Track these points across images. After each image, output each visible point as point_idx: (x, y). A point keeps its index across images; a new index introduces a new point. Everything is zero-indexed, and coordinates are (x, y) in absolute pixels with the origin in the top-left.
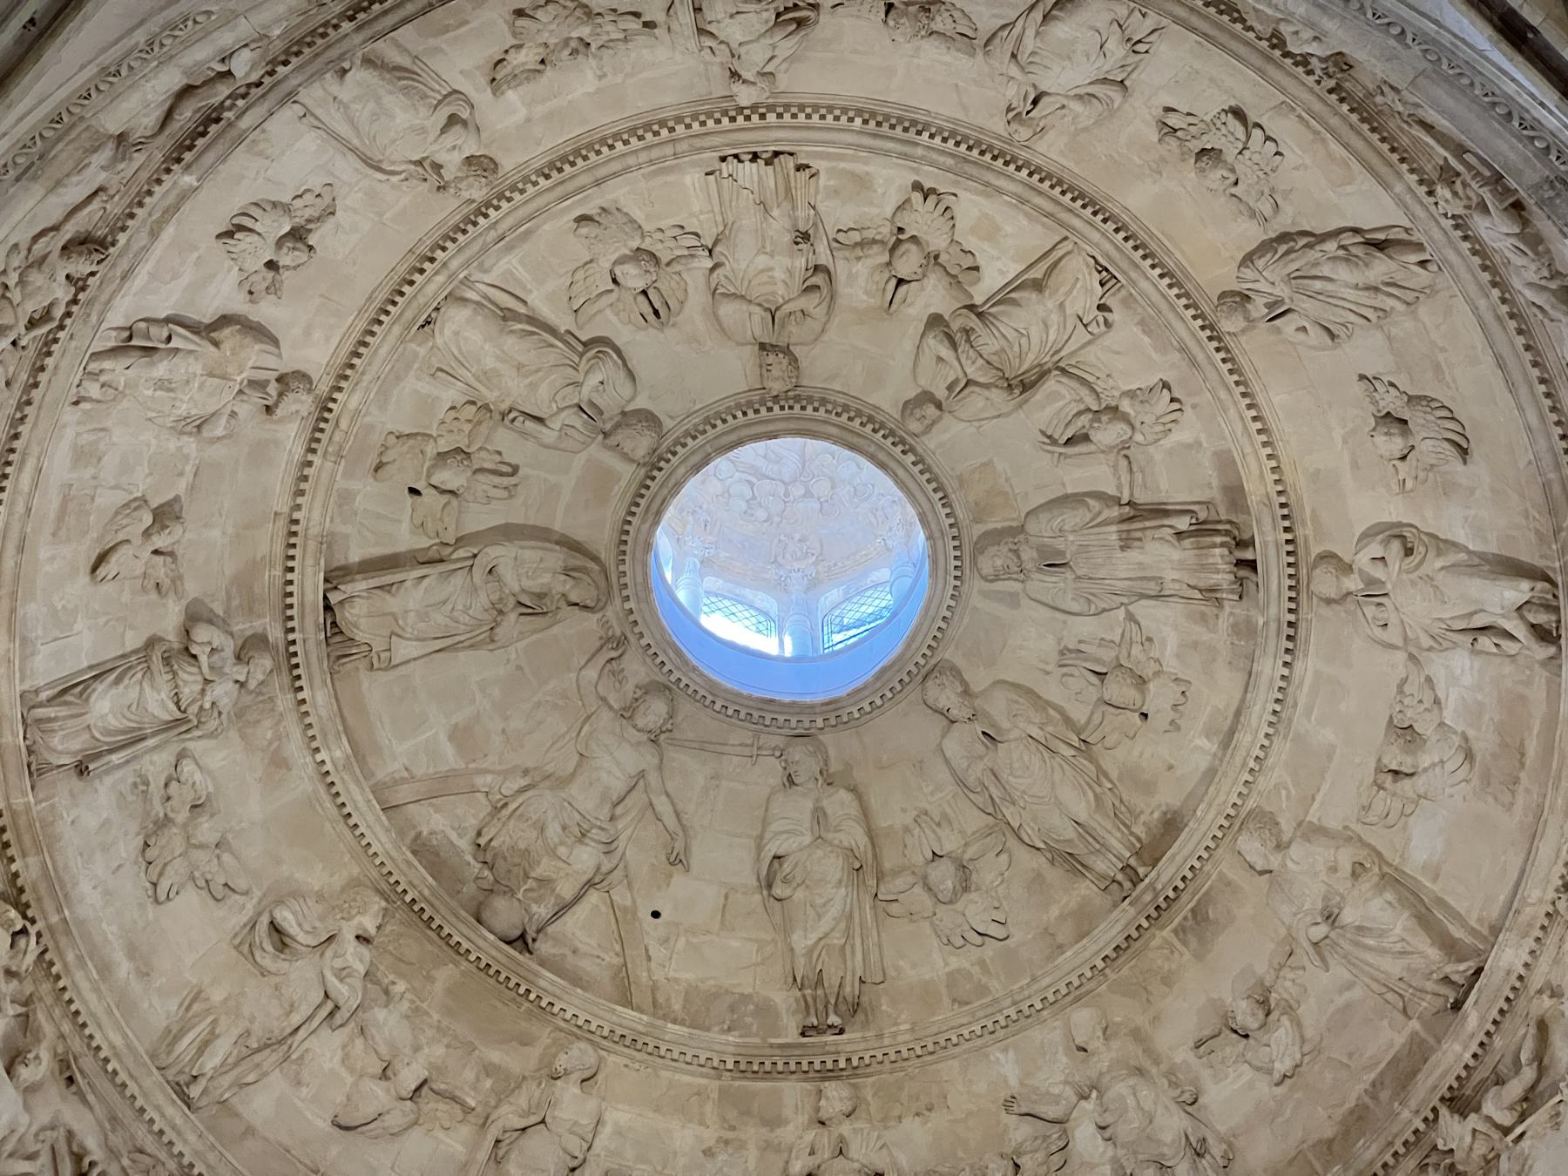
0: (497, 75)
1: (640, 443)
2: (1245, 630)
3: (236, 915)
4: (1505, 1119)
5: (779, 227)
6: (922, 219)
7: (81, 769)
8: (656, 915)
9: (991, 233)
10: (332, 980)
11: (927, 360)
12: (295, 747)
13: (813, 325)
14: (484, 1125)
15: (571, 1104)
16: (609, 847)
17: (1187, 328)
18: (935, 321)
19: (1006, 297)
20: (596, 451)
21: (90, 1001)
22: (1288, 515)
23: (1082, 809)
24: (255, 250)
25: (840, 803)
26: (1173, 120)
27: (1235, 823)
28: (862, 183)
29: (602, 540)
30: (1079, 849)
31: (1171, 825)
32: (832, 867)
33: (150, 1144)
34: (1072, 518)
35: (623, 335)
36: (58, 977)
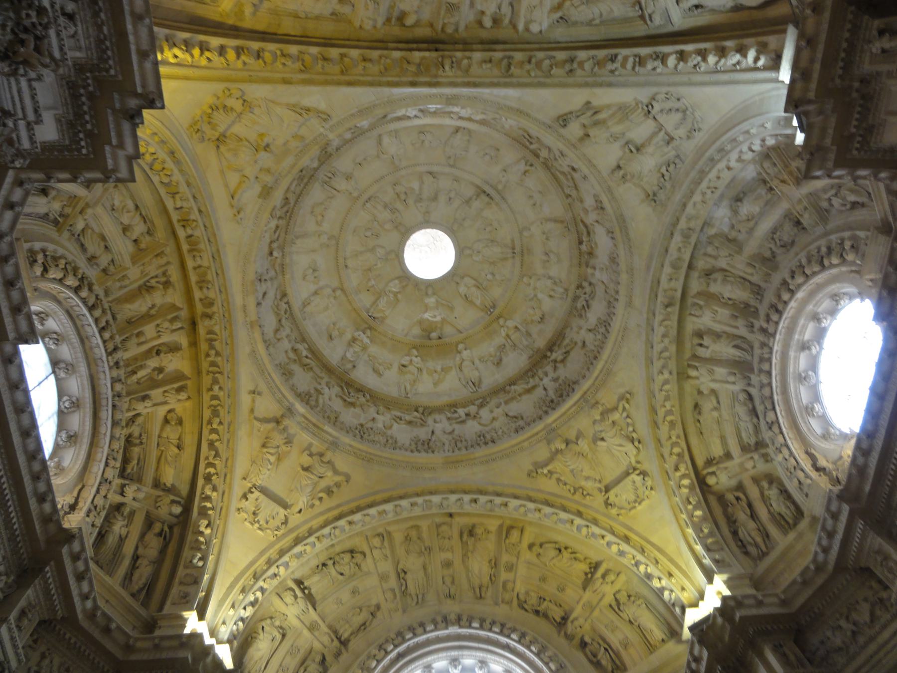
0: (318, 224)
1: (393, 256)
2: (497, 204)
4: (588, 239)
6: (399, 189)
10: (417, 365)
19: (421, 189)
22: (487, 182)
25: (467, 280)
27: (521, 233)
31: (513, 241)
32: (474, 289)
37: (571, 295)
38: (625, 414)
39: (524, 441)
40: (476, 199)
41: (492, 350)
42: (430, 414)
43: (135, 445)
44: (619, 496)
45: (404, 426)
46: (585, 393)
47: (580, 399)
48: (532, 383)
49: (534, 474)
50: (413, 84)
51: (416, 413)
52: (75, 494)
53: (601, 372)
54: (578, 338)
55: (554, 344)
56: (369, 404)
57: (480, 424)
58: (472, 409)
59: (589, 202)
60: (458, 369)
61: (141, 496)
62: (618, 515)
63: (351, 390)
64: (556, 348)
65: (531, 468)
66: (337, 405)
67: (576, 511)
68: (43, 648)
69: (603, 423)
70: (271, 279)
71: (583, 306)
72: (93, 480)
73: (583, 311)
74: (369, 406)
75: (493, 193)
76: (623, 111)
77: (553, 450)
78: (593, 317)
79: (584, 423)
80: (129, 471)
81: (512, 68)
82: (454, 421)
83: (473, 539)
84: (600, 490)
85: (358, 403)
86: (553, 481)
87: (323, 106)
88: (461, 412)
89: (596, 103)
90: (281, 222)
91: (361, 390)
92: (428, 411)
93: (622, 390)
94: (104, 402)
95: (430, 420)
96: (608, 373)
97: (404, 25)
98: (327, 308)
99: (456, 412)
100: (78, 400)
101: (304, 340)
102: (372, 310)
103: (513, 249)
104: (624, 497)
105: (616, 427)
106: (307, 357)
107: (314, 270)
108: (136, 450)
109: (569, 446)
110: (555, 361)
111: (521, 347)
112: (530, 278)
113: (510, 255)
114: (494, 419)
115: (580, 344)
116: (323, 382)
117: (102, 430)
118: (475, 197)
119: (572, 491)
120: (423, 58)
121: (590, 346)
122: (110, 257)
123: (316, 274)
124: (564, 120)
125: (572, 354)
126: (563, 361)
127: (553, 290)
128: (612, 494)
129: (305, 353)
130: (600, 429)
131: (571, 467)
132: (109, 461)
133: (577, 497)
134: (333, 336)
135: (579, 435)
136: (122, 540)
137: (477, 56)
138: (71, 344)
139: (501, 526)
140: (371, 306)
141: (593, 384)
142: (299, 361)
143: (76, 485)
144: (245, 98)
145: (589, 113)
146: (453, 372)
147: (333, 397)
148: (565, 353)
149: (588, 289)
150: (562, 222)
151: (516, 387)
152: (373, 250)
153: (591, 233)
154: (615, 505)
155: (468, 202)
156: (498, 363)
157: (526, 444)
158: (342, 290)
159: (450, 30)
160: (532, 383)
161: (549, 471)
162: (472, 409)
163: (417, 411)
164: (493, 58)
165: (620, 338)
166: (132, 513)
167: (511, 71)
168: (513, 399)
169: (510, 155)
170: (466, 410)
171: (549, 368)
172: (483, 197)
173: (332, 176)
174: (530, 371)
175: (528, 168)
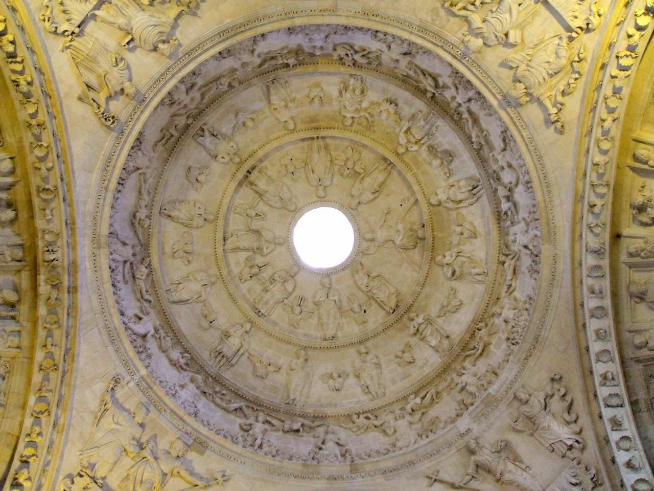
0: (278, 369)
2: (261, 161)
3: (455, 284)
4: (280, 59)
5: (266, 297)
6: (246, 276)
7: (448, 337)
8: (401, 205)
9: (238, 263)
11: (269, 250)
12: (423, 295)
13: (280, 273)
14: (458, 208)
15: (442, 196)
16: (397, 224)
17: (221, 222)
18: (262, 255)
20: (335, 286)
21: (483, 306)
23: (316, 155)
24: (338, 383)
26: (187, 263)
28: (249, 291)
29: (348, 271)
30: (323, 149)
31: (303, 140)
33: (499, 274)
34: (272, 204)
35: (310, 300)
36: (482, 315)
37: (353, 71)
38: (471, 7)
39: (522, 136)
40: (256, 185)
41: (436, 162)
42: (507, 246)
44: (577, 14)
45: (518, 282)
46: (454, 57)
47: (463, 64)
48: (466, 115)
49: (559, 125)
50: (73, 290)
51: (506, 265)
53: (425, 38)
54: (404, 62)
55: (417, 89)
56: (489, 325)
57: (517, 185)
58: (502, 192)
59: (229, 63)
60: (460, 205)
62: (600, 15)
63: (471, 346)
64: (421, 86)
65: (552, 128)
66: (482, 366)
67: (602, 71)
69: (486, 35)
70: (327, 433)
71: (363, 56)
73: (370, 56)
74: (492, 325)
75: (246, 167)
76: (81, 62)
77: (528, 99)
78: (374, 46)
79: (493, 58)
81: (47, 187)
82: (516, 217)
83: (649, 209)
84: (571, 39)
85: (486, 338)
86: (566, 100)
87: (100, 387)
88: (505, 206)
89: (78, 90)
90: (261, 418)
91: (473, 333)
92: (505, 251)
93: (442, 13)
95: (515, 248)
96: (423, 30)
97: (19, 301)
98: (378, 365)
99: (506, 213)
101: (405, 398)
102: (387, 308)
103: (313, 138)
104: (577, 7)
105: (489, 18)
106: (423, 398)
107: (331, 377)
109: (522, 79)
110: (437, 86)
111: (427, 127)
112: (345, 117)
113: (321, 142)
114: (510, 166)
115: (408, 58)
116: (457, 379)
118: (254, 187)
119: (577, 76)
120: (46, 282)
121: (405, 48)
123: (335, 375)
124: (108, 119)
125: (424, 67)
126: (435, 79)
127: (354, 90)
128: (574, 24)
129: (418, 400)
130: (494, 38)
131: (546, 77)
133: (584, 67)
134: (411, 360)
135: (504, 64)
137: (40, 224)
139: (634, 169)
140: (384, 309)
141: (442, 47)
142: (423, 410)
144: (75, 473)
145: (92, 94)
146: (464, 211)
147: (474, 369)
148: (425, 75)
149: (341, 52)
150: (268, 88)
151: (473, 135)
152: (317, 304)
153: (271, 55)
154: (587, 19)
155: (260, 195)
156: (450, 155)
157: (524, 134)
158: (360, 343)
159: (19, 254)
160: (466, 115)
161: (554, 106)
162: (502, 192)
163: (504, 263)
164: (41, 207)
165: (377, 19)
167: (52, 189)
168: (487, 141)
169: (192, 154)
170: (503, 201)
171: (448, 94)
172: (252, 177)
173: (221, 355)
174: (454, 117)
175: (207, 133)
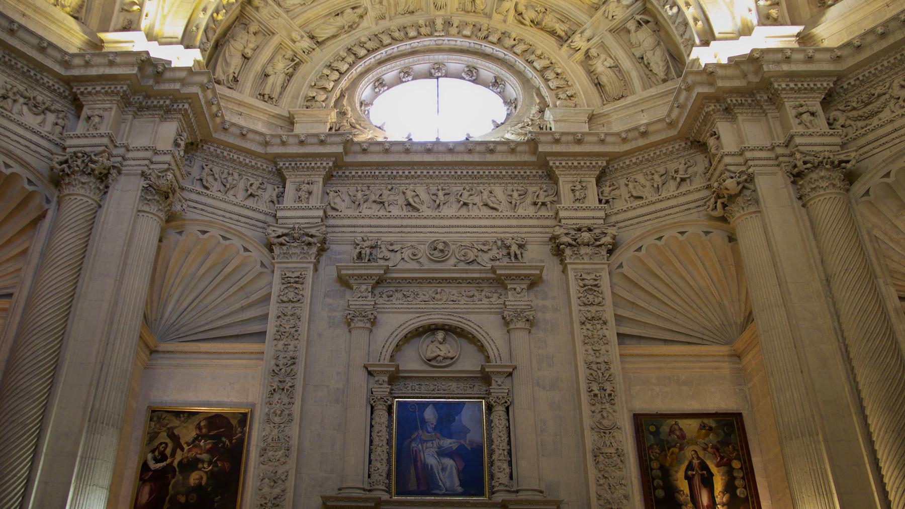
43: (542, 20)
52: (538, 101)
61: (588, 34)
68: (623, 182)
72: (538, 81)
80: (563, 34)
94: (477, 47)
100: (468, 66)
108: (549, 21)
117: (501, 55)
122: (349, 11)
132: (529, 60)
136: (616, 68)
138: (414, 61)
143: (532, 97)
166: (603, 45)
